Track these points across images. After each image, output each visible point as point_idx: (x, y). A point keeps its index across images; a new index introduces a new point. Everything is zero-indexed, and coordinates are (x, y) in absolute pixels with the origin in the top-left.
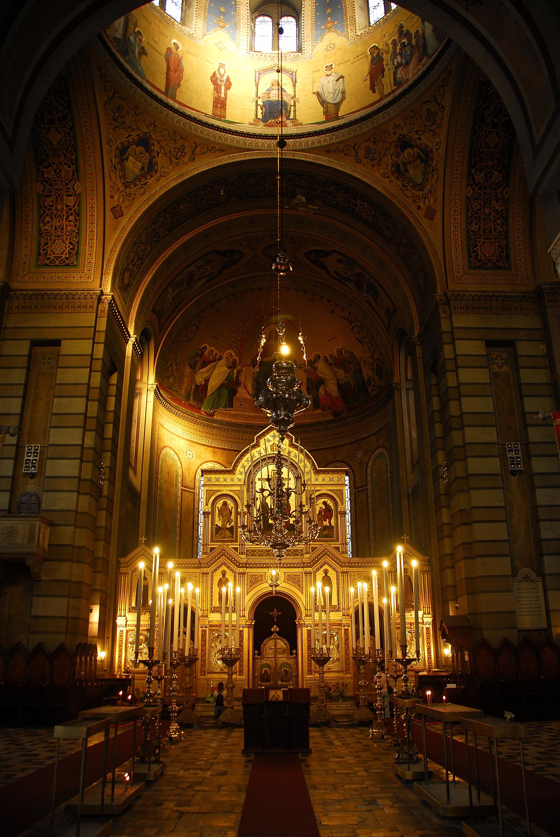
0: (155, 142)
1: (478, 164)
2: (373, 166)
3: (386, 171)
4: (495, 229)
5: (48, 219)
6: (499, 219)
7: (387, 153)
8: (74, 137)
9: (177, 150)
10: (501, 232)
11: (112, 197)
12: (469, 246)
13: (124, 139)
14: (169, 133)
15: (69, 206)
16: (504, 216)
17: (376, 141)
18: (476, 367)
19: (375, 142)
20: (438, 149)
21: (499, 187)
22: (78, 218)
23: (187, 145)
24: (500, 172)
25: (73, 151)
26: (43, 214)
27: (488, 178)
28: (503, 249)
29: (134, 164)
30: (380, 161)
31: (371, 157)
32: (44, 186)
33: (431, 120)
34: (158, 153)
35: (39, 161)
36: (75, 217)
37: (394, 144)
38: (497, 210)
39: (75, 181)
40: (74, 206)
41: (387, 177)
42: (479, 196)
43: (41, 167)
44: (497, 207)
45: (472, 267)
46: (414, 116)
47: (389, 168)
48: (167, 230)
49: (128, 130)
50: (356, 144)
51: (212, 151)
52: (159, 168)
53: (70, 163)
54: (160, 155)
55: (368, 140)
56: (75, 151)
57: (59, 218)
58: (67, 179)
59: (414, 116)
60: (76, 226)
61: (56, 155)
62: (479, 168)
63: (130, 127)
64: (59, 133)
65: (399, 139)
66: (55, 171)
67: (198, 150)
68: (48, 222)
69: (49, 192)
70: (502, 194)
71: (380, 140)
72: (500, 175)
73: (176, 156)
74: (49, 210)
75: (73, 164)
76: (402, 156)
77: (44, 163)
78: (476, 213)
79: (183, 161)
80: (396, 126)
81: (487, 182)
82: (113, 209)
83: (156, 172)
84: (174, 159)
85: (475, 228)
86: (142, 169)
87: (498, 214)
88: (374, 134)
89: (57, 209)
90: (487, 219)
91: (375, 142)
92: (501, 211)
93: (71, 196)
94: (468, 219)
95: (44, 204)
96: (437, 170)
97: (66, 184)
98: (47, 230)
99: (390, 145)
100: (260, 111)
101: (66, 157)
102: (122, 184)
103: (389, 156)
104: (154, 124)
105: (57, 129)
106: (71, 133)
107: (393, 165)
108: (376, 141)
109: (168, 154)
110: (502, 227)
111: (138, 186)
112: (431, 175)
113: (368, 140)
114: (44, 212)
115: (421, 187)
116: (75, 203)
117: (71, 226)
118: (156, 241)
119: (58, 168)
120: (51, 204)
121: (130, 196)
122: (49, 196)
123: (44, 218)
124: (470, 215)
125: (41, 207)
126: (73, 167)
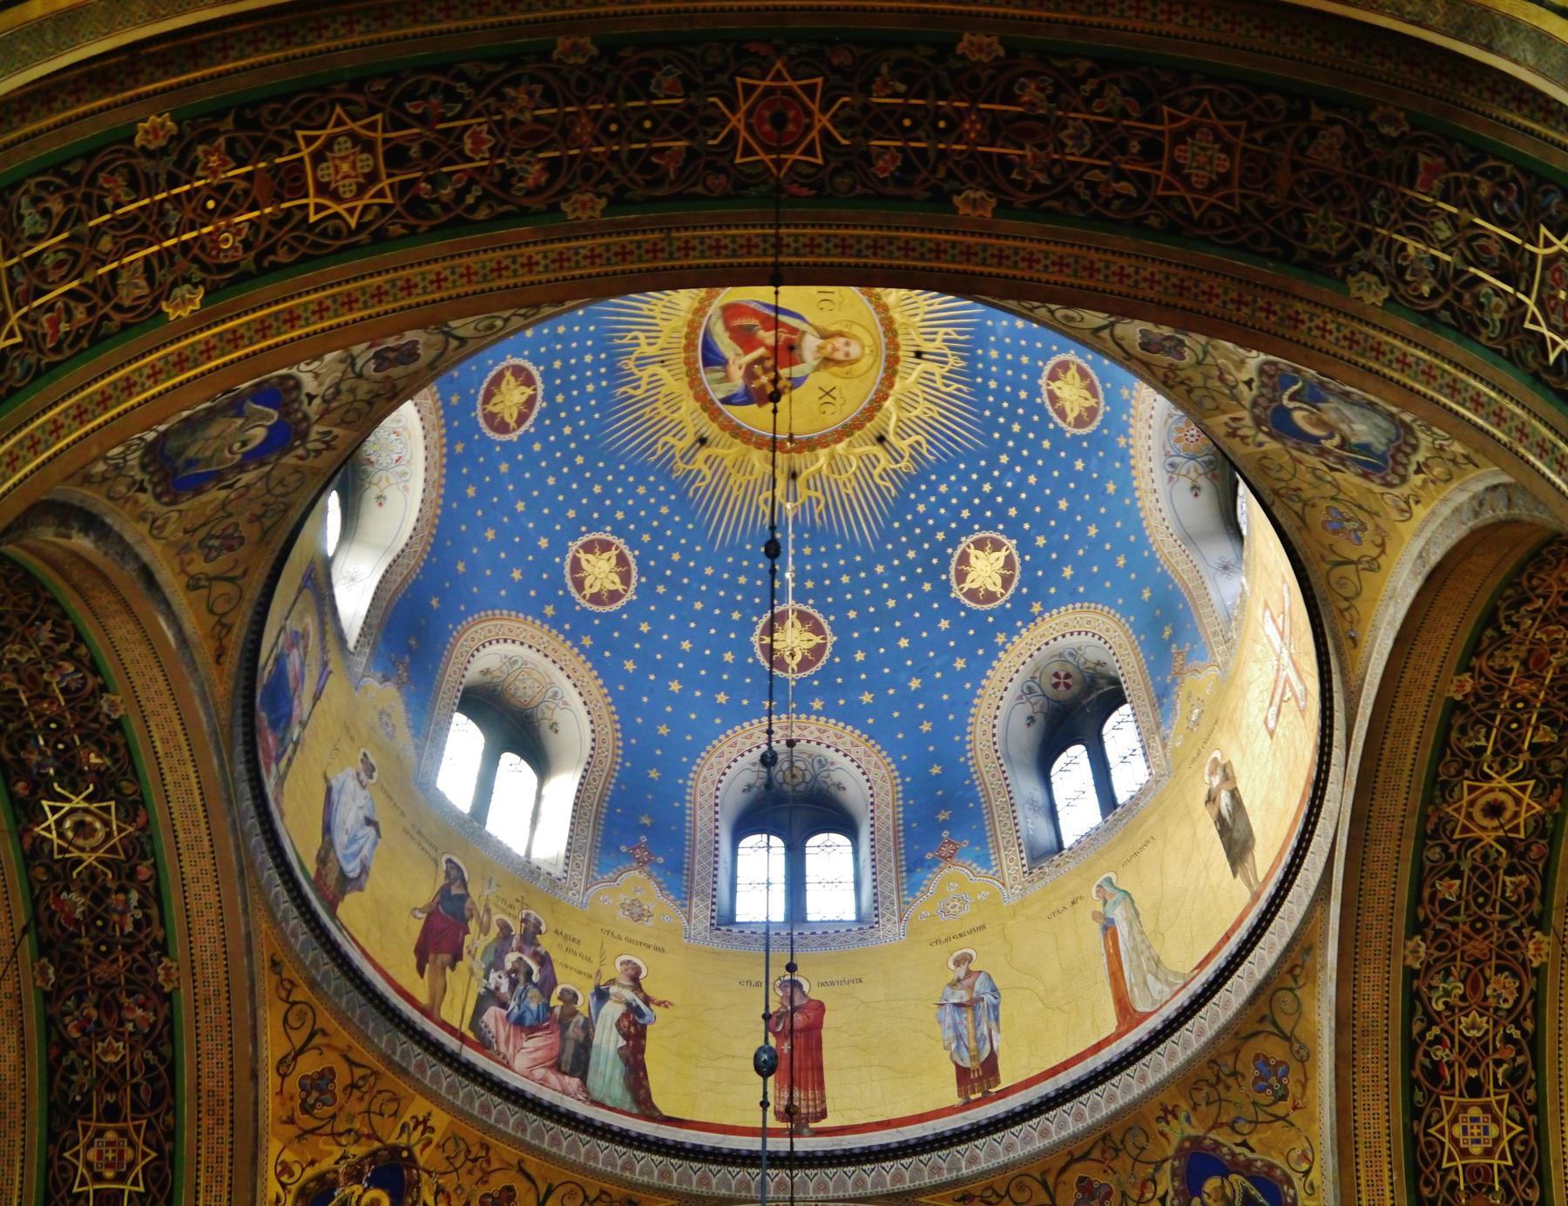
2: (291, 1121)
3: (297, 1169)
5: (56, 206)
7: (343, 1141)
8: (353, 246)
15: (115, 287)
17: (359, 1088)
19: (353, 1086)
22: (84, 344)
25: (302, 250)
26: (65, 176)
30: (313, 1131)
31: (311, 1100)
32: (163, 151)
34: (230, 486)
35: (248, 114)
36: (86, 327)
37: (377, 1144)
39: (203, 282)
40: (119, 308)
41: (283, 1185)
43: (229, 123)
46: (475, 1160)
47: (310, 1172)
50: (324, 1033)
51: (218, 628)
53: (260, 245)
55: (352, 1063)
56: (305, 258)
57: (71, 259)
58: (203, 248)
59: (475, 1160)
60: (56, 350)
61: (281, 184)
64: (361, 191)
65: (395, 1150)
66: (223, 188)
68: (46, 213)
69: (146, 175)
71: (367, 1098)
74: (87, 198)
75: (259, 259)
77: (242, 135)
80: (424, 1123)
88: (375, 1073)
93: (150, 280)
95: (101, 168)
98: (21, 218)
99: (369, 1137)
101: (278, 222)
103: (338, 1153)
105: (372, 177)
106: (363, 237)
107: (320, 1178)
108: (359, 1088)
109: (221, 514)
113: (352, 1063)
114: (75, 180)
116: (131, 309)
117: (54, 324)
119: (234, 198)
120: (109, 202)
123: (59, 188)
125: (88, 156)
126: (248, 262)
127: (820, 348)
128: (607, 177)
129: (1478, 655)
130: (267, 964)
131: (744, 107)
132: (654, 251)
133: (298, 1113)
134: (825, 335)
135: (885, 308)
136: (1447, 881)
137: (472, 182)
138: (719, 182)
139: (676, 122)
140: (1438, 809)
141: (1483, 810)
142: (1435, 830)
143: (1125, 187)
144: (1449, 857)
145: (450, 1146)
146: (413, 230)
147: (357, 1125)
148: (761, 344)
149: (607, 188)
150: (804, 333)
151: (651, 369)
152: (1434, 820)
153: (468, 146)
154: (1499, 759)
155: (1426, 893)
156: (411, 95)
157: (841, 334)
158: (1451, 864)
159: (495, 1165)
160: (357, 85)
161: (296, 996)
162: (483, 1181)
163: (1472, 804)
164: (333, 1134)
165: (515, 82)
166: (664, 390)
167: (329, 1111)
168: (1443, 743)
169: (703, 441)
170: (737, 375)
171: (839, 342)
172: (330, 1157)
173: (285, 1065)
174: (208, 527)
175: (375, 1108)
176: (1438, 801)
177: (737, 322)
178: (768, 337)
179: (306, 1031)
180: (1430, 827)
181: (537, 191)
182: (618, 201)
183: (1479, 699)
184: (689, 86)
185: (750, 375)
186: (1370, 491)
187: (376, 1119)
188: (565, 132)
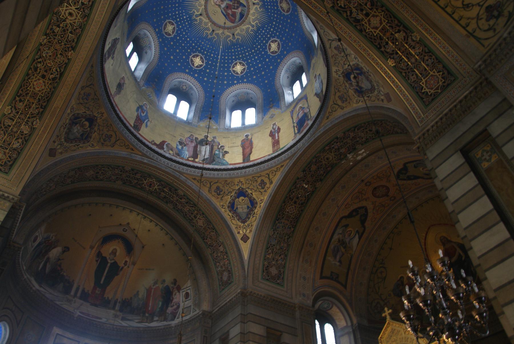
0: (247, 189)
1: (382, 42)
2: (349, 103)
3: (356, 98)
4: (427, 65)
6: (425, 56)
9: (260, 185)
10: (433, 63)
11: (239, 233)
12: (417, 93)
13: (229, 200)
14: (251, 180)
16: (427, 51)
18: (461, 179)
19: (339, 91)
20: (358, 61)
21: (407, 40)
23: (263, 178)
24: (399, 31)
27: (396, 42)
28: (443, 71)
29: (242, 208)
31: (345, 100)
33: (341, 51)
34: (252, 193)
38: (419, 53)
41: (359, 101)
42: (400, 58)
44: (418, 51)
45: (428, 105)
46: (335, 58)
47: (355, 96)
48: (290, 228)
49: (229, 194)
50: (333, 102)
52: (257, 199)
54: (253, 193)
55: (335, 93)
59: (335, 58)
62: (385, 44)
63: (229, 192)
66: (210, 238)
67: (271, 176)
70: (414, 41)
72: (402, 32)
73: (262, 187)
75: (213, 229)
76: (353, 83)
78: (408, 69)
79: (267, 187)
81: (397, 45)
82: (242, 239)
83: (257, 203)
84: (262, 190)
85: (414, 78)
86: (248, 207)
87: (422, 55)
88: (335, 87)
89: (219, 257)
90: (417, 65)
91: (339, 91)
92: (422, 51)
93: (220, 245)
94: (405, 78)
96: (368, 70)
97: (217, 241)
100: (296, 129)
102: (241, 222)
103: (350, 90)
104: (240, 181)
106: (204, 216)
107: (355, 92)
110: (431, 59)
111: (251, 217)
112: (370, 77)
115: (372, 90)
118: (288, 239)
121: (249, 226)
122: (214, 252)
124: (404, 74)
127: (222, 4)
128: (176, 193)
129: (66, 63)
130: (328, 120)
131: (155, 188)
132: (176, 182)
133: (348, 102)
134: (219, 6)
135: (205, 6)
136: (85, 3)
137: (191, 206)
138: (163, 183)
139: (164, 191)
140: (84, 22)
141: (73, 16)
142: (85, 17)
143: (102, 169)
144: (83, 8)
145: (337, 65)
146: (200, 210)
147: (344, 87)
148: (232, 12)
149: (176, 192)
150: (223, 8)
151: (253, 23)
152: (85, 20)
153: (188, 209)
154: (67, 28)
155: (91, 3)
156: (189, 219)
157: (216, 5)
158: (83, 6)
159: (333, 54)
160: (193, 226)
161: (331, 111)
162: (337, 55)
163: (75, 19)
164: (348, 92)
165: (179, 209)
166: (253, 18)
167: (345, 95)
168: (78, 39)
169: (254, 4)
170: (240, 9)
171: (218, 3)
172: (351, 92)
173: (342, 108)
174: (260, 190)
175: (339, 84)
176: (83, 24)
177: (233, 19)
178: (230, 12)
179: (335, 106)
180: (86, 18)
181: (184, 199)
182: (176, 190)
183: (68, 48)
184: (160, 194)
185: (238, 8)
186: (78, 110)
187: (341, 83)
188: (177, 201)
